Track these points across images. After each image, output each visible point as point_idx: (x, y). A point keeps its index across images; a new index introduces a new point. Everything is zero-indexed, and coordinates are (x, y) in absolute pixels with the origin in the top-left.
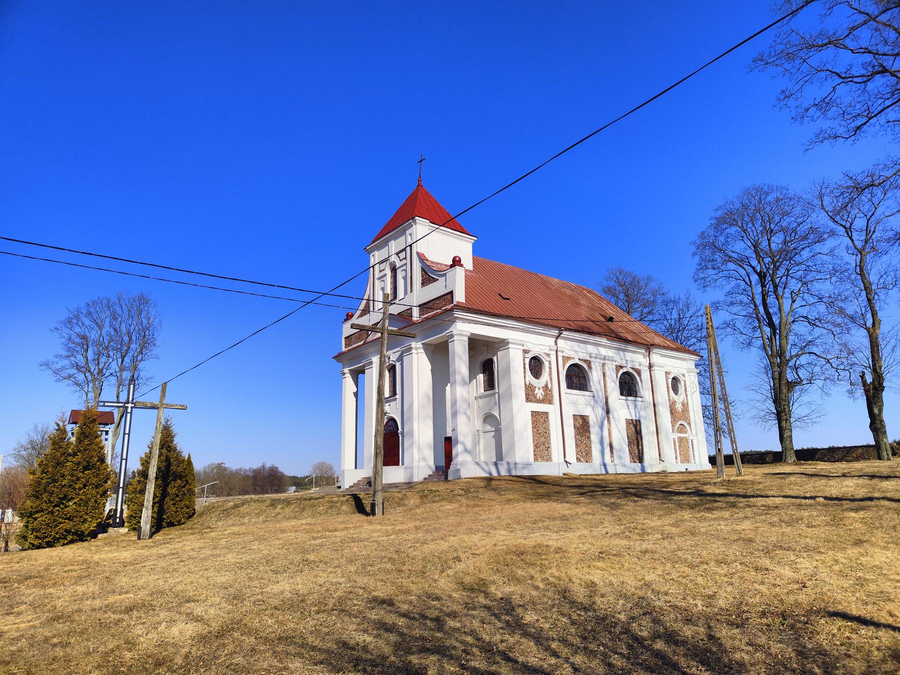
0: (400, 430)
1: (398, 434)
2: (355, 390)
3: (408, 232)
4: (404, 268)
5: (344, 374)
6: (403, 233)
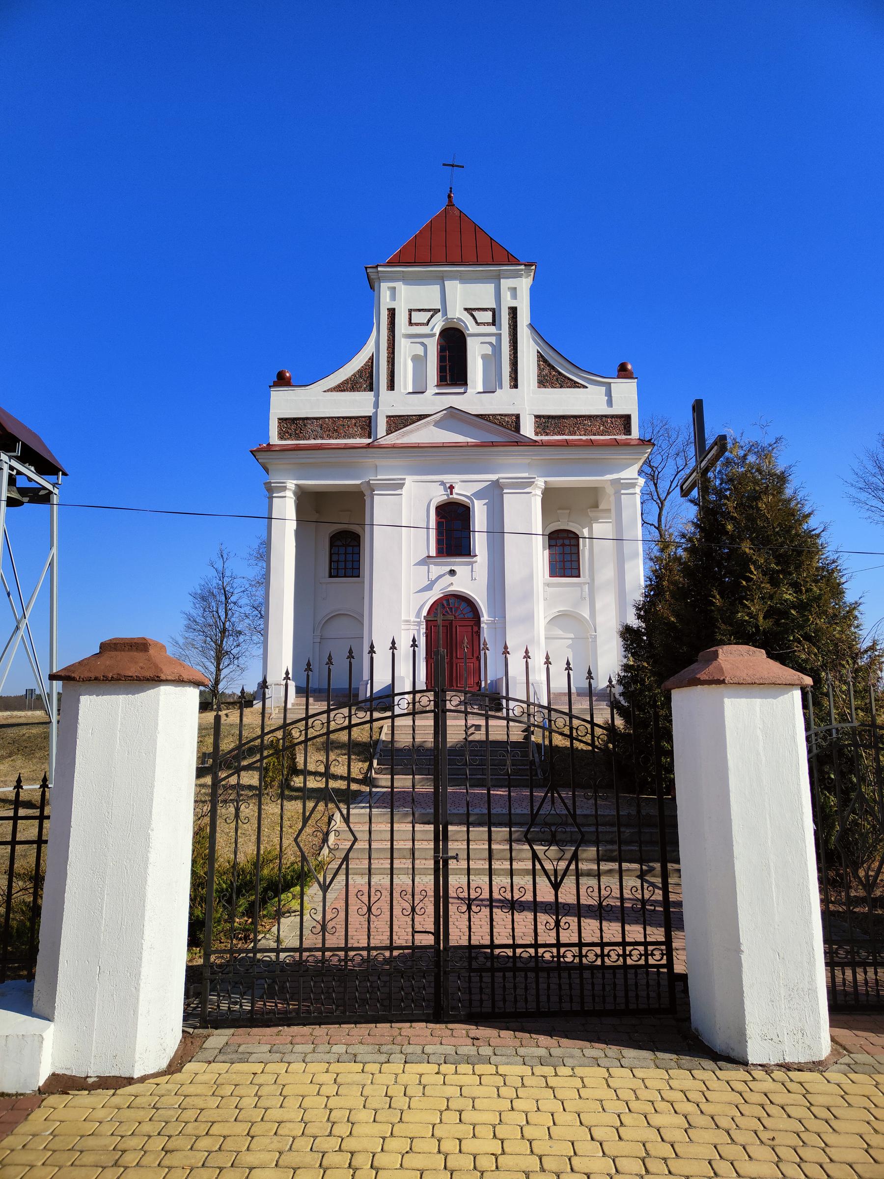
0: (485, 618)
5: (284, 489)
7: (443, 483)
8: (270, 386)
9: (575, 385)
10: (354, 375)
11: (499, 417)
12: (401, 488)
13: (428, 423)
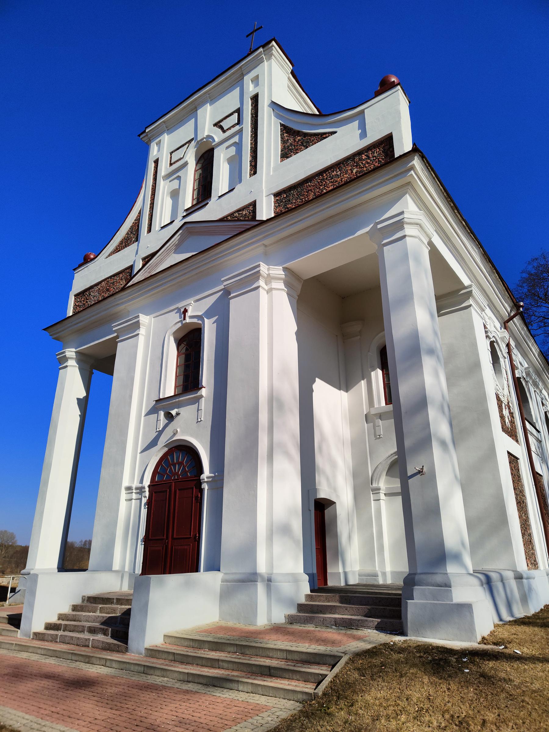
0: (207, 473)
1: (199, 483)
2: (82, 394)
3: (247, 79)
4: (236, 139)
5: (65, 359)
6: (239, 81)
7: (179, 309)
8: (74, 270)
9: (322, 136)
10: (127, 234)
11: (236, 214)
12: (139, 327)
13: (169, 249)
